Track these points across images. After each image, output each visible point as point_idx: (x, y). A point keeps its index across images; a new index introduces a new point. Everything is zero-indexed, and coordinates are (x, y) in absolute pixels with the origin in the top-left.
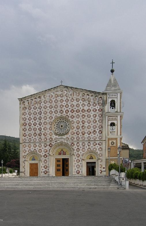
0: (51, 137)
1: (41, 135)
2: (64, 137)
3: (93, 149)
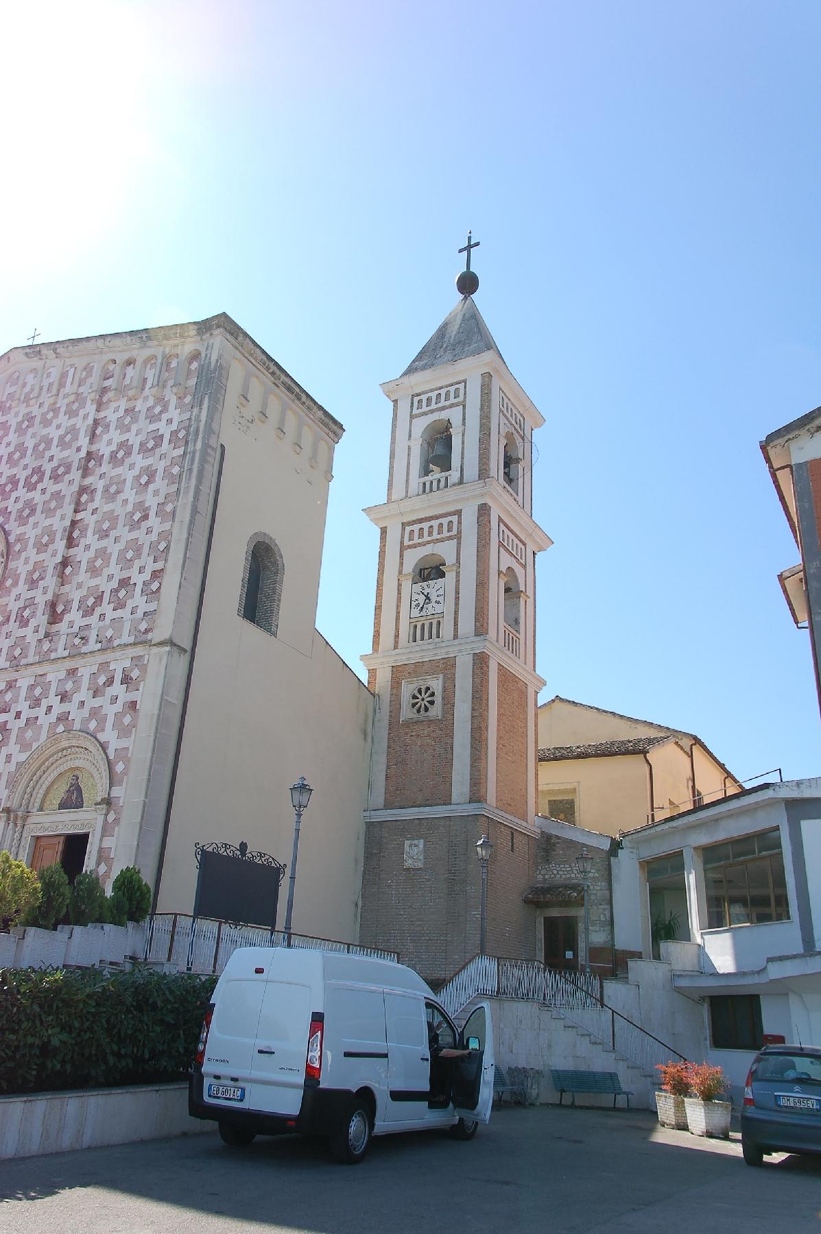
3: (86, 721)
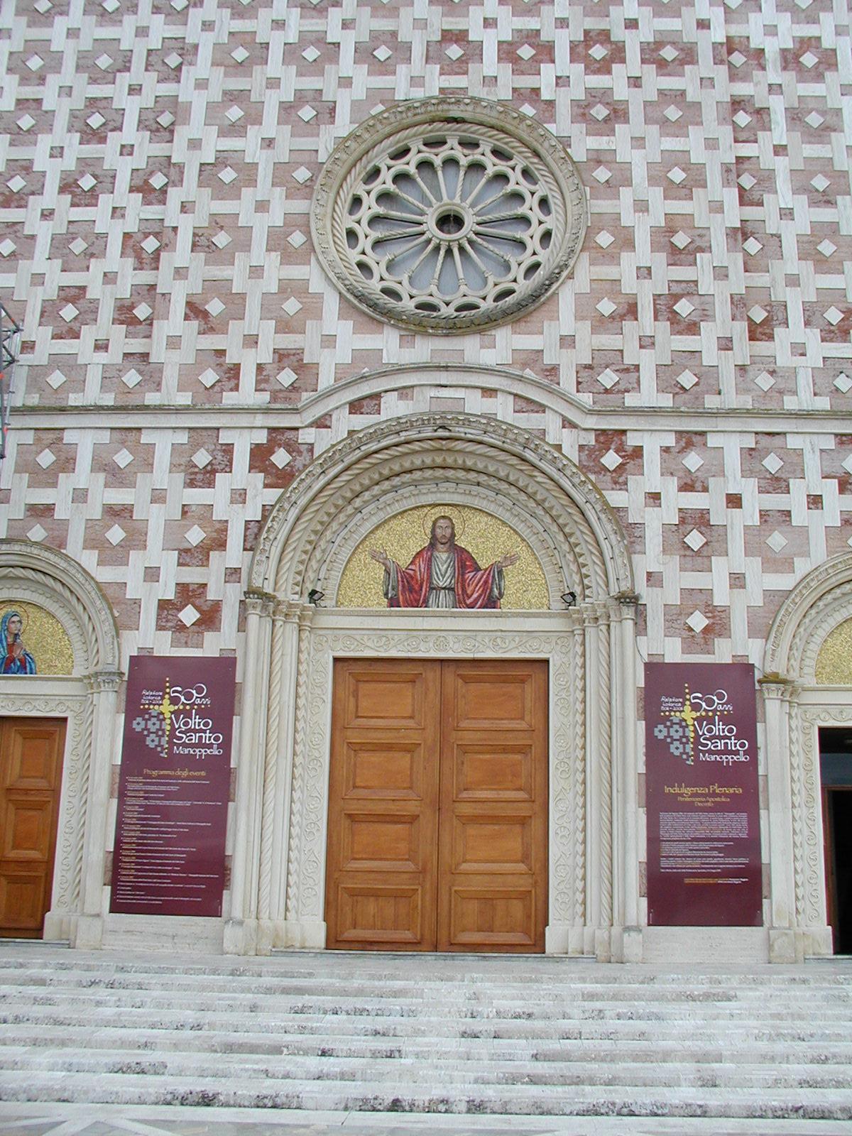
0: (288, 341)
1: (150, 321)
2: (489, 357)
